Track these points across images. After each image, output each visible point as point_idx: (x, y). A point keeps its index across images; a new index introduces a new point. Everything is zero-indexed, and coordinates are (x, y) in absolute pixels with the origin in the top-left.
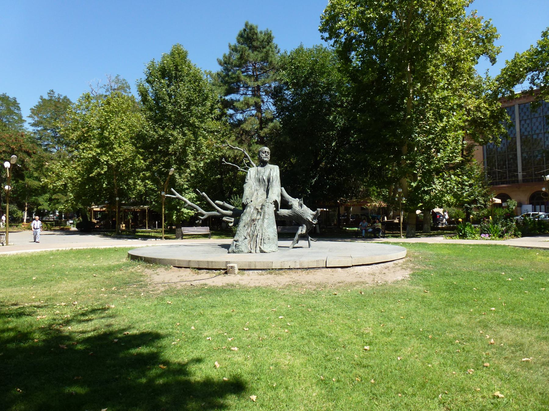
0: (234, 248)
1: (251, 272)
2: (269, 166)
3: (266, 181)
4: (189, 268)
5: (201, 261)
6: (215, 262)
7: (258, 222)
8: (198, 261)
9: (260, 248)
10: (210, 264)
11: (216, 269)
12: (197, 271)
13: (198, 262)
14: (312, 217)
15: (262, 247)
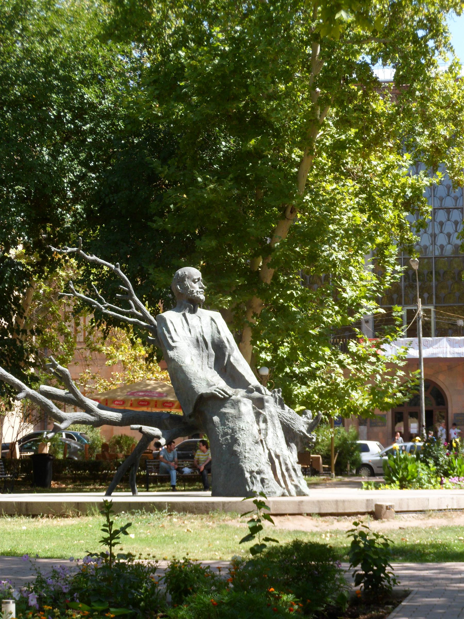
0: (261, 485)
1: (405, 515)
2: (205, 314)
3: (210, 345)
4: (301, 514)
5: (324, 501)
6: (349, 501)
7: (266, 434)
8: (318, 502)
9: (296, 486)
10: (341, 505)
11: (349, 515)
12: (321, 519)
13: (319, 502)
14: (306, 426)
15: (299, 485)
